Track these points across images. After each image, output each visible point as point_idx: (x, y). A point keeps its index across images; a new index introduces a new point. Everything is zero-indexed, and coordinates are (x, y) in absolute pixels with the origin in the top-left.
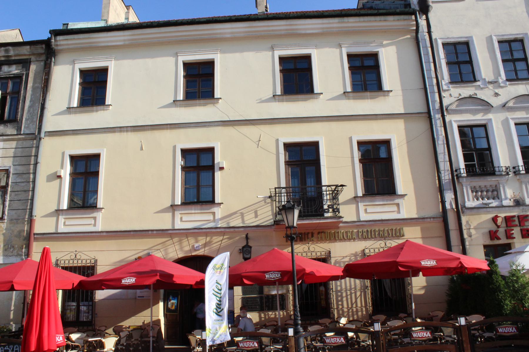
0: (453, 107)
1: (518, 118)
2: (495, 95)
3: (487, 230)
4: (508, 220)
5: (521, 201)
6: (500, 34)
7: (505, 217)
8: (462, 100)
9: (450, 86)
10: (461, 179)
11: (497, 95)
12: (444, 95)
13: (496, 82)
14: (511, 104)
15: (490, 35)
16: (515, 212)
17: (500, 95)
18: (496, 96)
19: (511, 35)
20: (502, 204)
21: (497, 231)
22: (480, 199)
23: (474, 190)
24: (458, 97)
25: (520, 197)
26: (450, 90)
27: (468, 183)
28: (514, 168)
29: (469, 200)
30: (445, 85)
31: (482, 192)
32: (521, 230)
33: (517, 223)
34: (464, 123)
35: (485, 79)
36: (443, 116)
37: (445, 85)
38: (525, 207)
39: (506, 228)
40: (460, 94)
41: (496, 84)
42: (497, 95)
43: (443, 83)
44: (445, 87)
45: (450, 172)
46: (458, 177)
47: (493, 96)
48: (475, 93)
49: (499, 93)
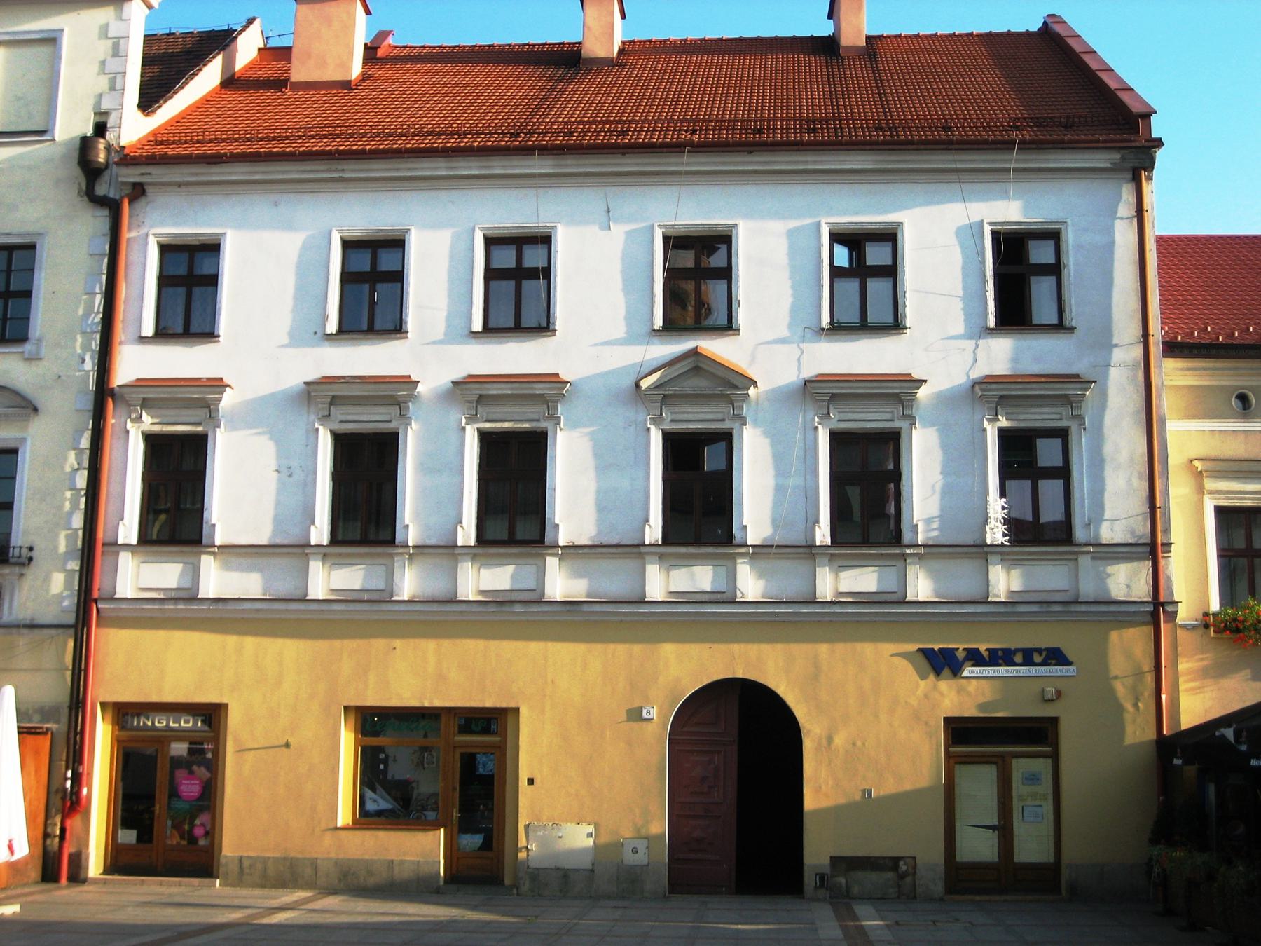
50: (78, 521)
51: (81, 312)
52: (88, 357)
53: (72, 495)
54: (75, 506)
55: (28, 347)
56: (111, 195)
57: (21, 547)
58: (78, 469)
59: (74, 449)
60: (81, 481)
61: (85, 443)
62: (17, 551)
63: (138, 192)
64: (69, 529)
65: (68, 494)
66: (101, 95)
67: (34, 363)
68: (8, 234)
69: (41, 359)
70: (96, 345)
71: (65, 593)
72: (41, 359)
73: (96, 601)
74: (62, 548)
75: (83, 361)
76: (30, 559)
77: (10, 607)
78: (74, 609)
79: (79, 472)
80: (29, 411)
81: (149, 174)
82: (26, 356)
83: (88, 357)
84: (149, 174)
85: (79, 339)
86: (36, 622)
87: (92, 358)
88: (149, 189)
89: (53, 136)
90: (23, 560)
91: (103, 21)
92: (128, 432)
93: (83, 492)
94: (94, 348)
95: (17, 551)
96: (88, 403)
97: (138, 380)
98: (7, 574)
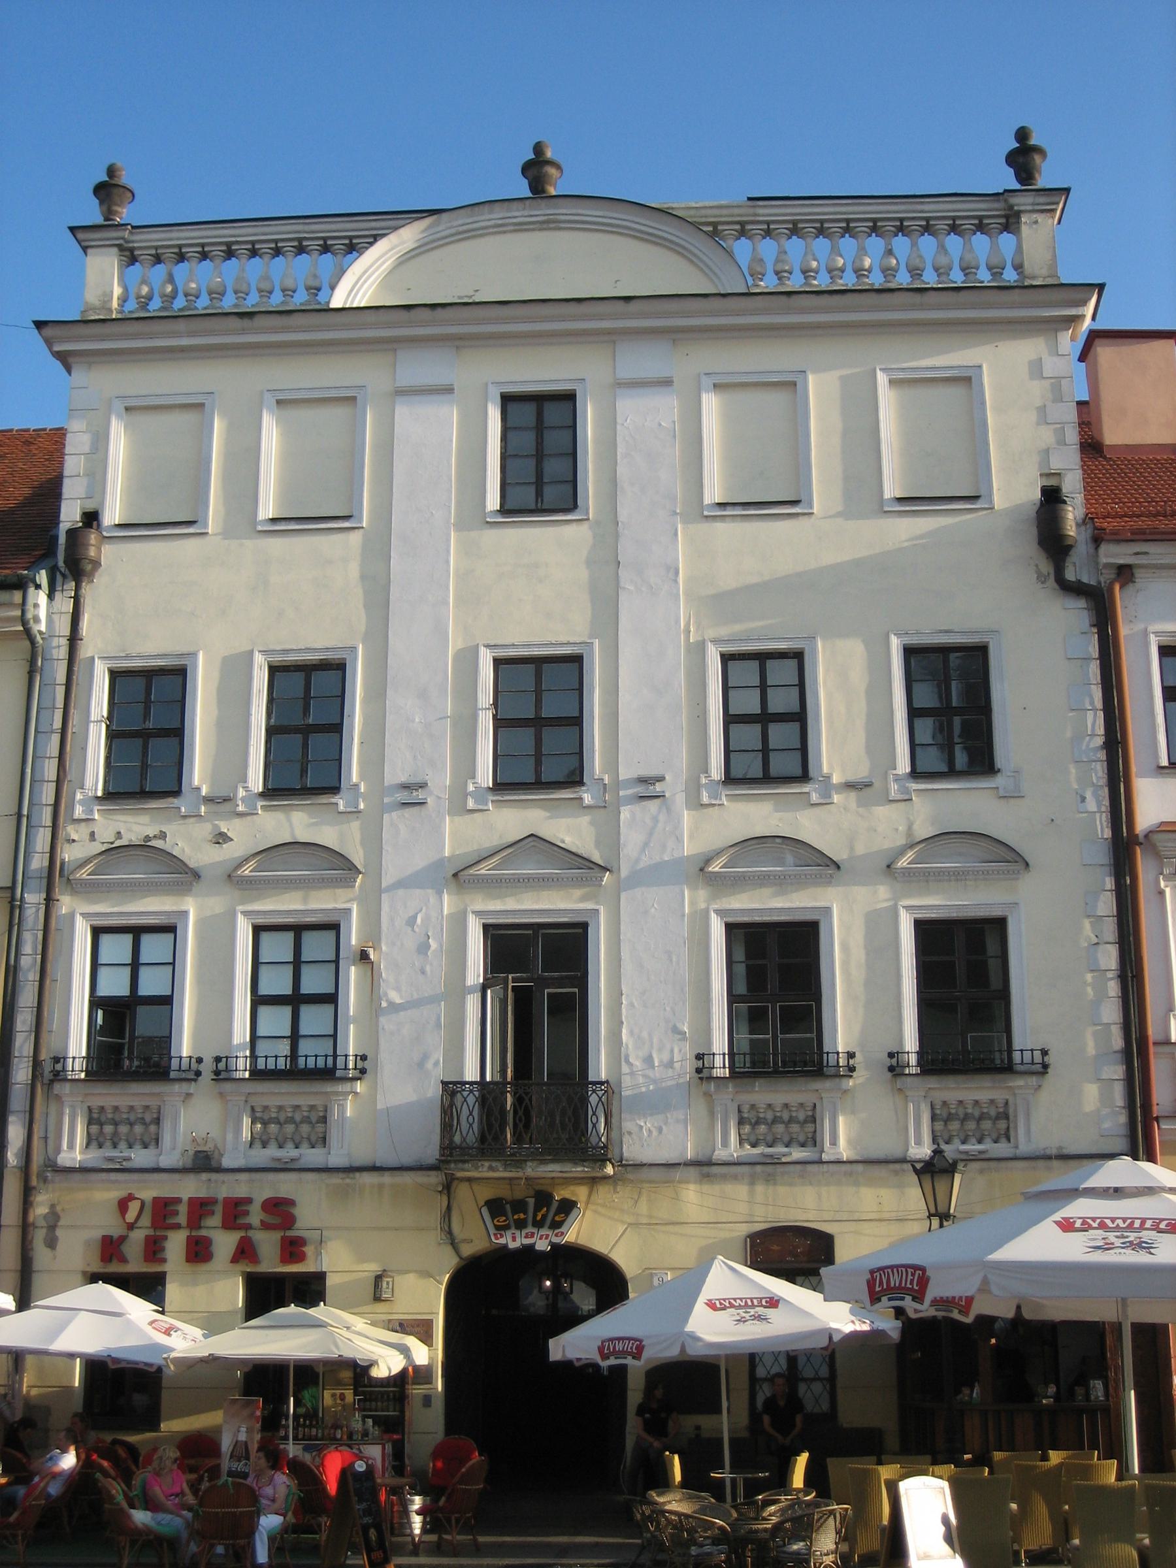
0: (83, 874)
1: (265, 913)
2: (214, 840)
3: (98, 1234)
4: (163, 1209)
5: (216, 1155)
6: (278, 648)
7: (156, 1200)
8: (115, 852)
9: (96, 808)
10: (58, 1088)
11: (221, 838)
12: (74, 836)
13: (226, 800)
14: (246, 871)
15: (250, 648)
16: (189, 1188)
17: (232, 840)
18: (218, 843)
19: (308, 650)
20: (158, 1163)
21: (123, 1239)
22: (108, 1144)
23: (94, 1119)
24: (112, 843)
25: (216, 1147)
26: (94, 820)
27: (80, 1099)
28: (218, 1059)
29: (71, 1146)
30: (81, 802)
31: (116, 1124)
32: (190, 1239)
33: (182, 1219)
34: (111, 922)
35: (198, 789)
36: (49, 901)
37: (81, 802)
38: (214, 1176)
39: (151, 1232)
40: (119, 833)
41: (227, 807)
42: (221, 838)
43: (79, 796)
44: (79, 812)
45: (31, 1064)
46: (58, 1076)
47: (211, 841)
48: (161, 831)
49: (229, 834)
50: (1111, 1013)
51: (1069, 734)
52: (1089, 795)
53: (1093, 977)
54: (1101, 995)
55: (999, 781)
56: (1085, 580)
57: (1032, 1050)
58: (1097, 944)
59: (1089, 916)
60: (1110, 958)
61: (1106, 904)
62: (1027, 1055)
63: (1125, 573)
64: (1095, 1025)
65: (1089, 977)
66: (1047, 451)
67: (1012, 801)
68: (947, 632)
69: (1023, 797)
70: (1098, 778)
71: (1105, 1111)
72: (1023, 797)
73: (1157, 1119)
74: (1091, 1049)
75: (1083, 799)
76: (1045, 1066)
77: (1028, 1131)
78: (1124, 1131)
79: (1101, 947)
80: (1021, 866)
81: (1146, 553)
82: (1002, 793)
83: (1089, 795)
84: (1146, 553)
85: (1073, 770)
86: (1065, 1152)
87: (1095, 794)
88: (1138, 573)
89: (991, 501)
90: (1038, 1068)
91: (1033, 356)
92: (1161, 893)
93: (1110, 975)
94: (1095, 781)
95: (1027, 1055)
96: (1101, 855)
97: (1162, 823)
98: (1020, 1087)
